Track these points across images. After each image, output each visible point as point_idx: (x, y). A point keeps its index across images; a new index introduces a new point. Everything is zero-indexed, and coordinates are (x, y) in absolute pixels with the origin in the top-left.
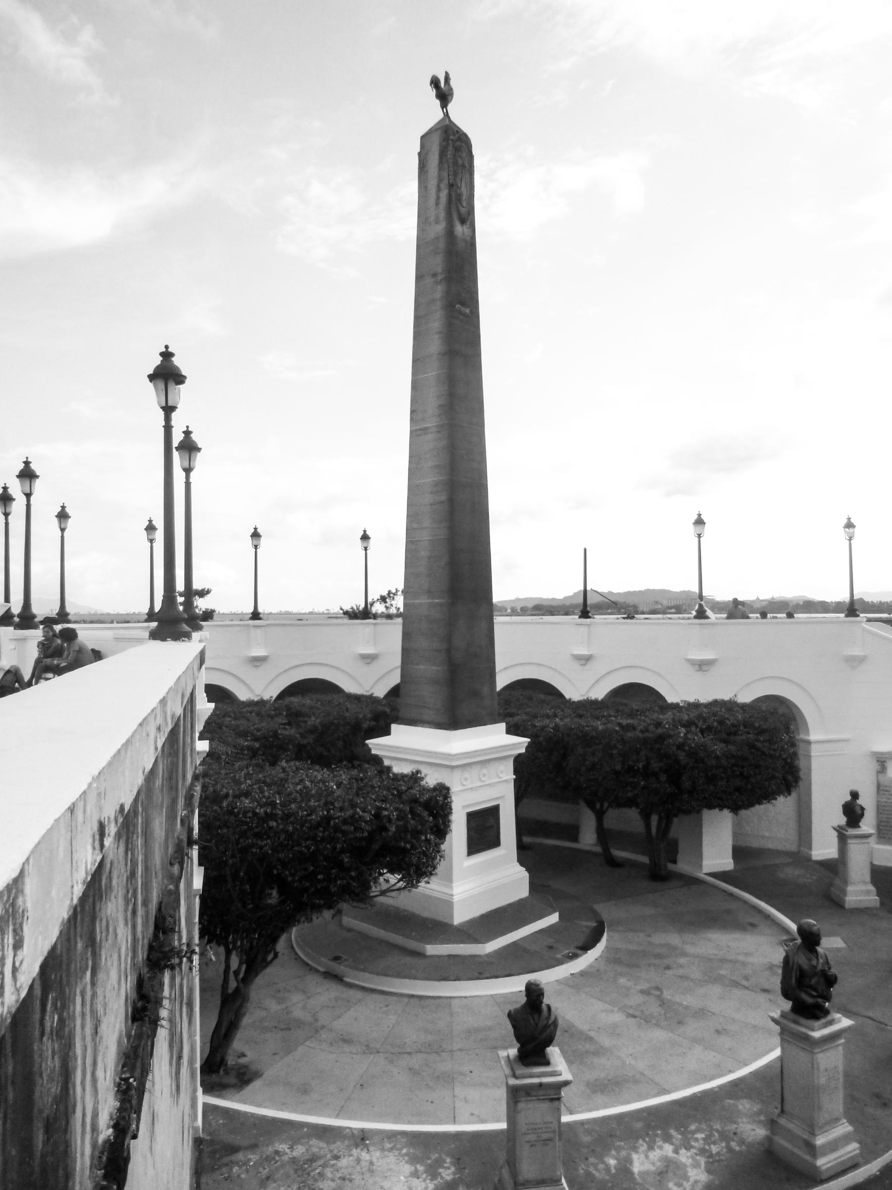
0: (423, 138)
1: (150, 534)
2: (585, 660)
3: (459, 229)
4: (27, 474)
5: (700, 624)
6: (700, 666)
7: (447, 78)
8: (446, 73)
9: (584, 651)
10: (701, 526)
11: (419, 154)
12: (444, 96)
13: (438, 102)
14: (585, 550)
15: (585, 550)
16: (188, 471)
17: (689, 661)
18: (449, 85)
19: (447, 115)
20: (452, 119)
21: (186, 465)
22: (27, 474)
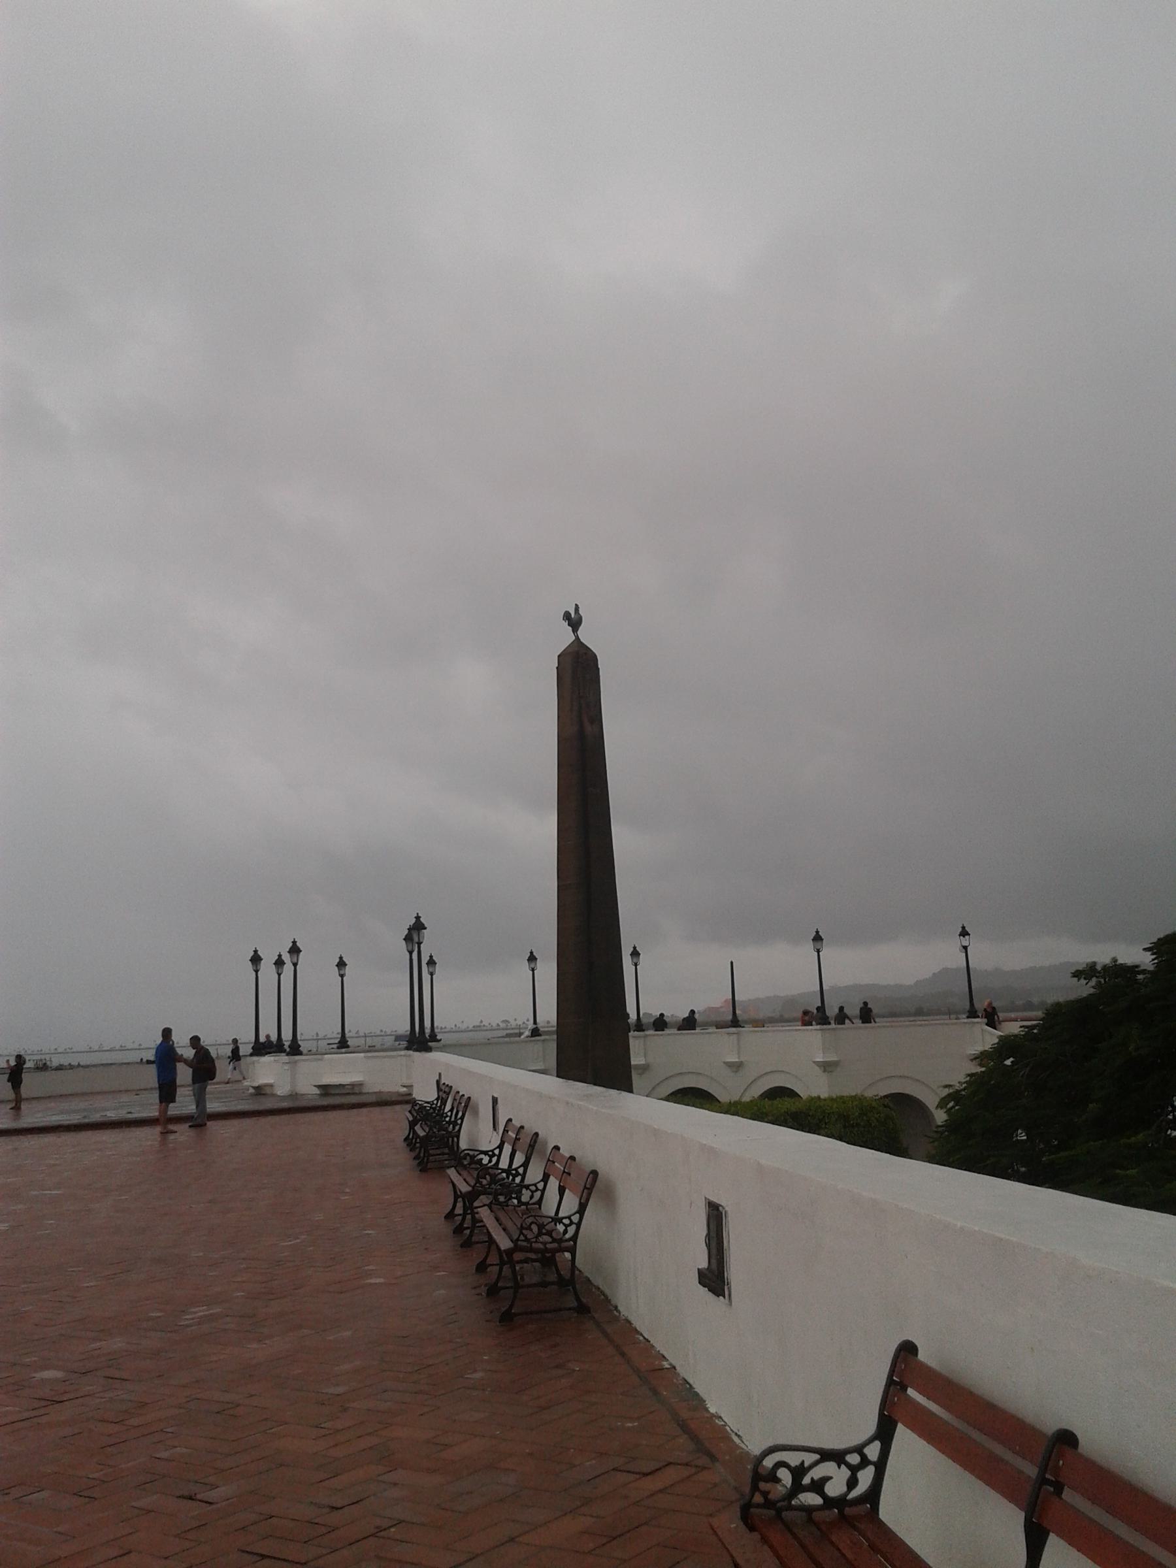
0: (559, 656)
1: (341, 970)
2: (737, 1067)
3: (588, 728)
4: (295, 950)
5: (821, 1030)
6: (824, 1067)
7: (577, 608)
8: (576, 605)
9: (733, 1059)
10: (820, 943)
11: (557, 668)
12: (574, 622)
13: (570, 628)
14: (732, 963)
15: (732, 963)
16: (432, 974)
17: (814, 1062)
18: (579, 614)
19: (577, 638)
20: (582, 640)
21: (410, 949)
22: (295, 950)
